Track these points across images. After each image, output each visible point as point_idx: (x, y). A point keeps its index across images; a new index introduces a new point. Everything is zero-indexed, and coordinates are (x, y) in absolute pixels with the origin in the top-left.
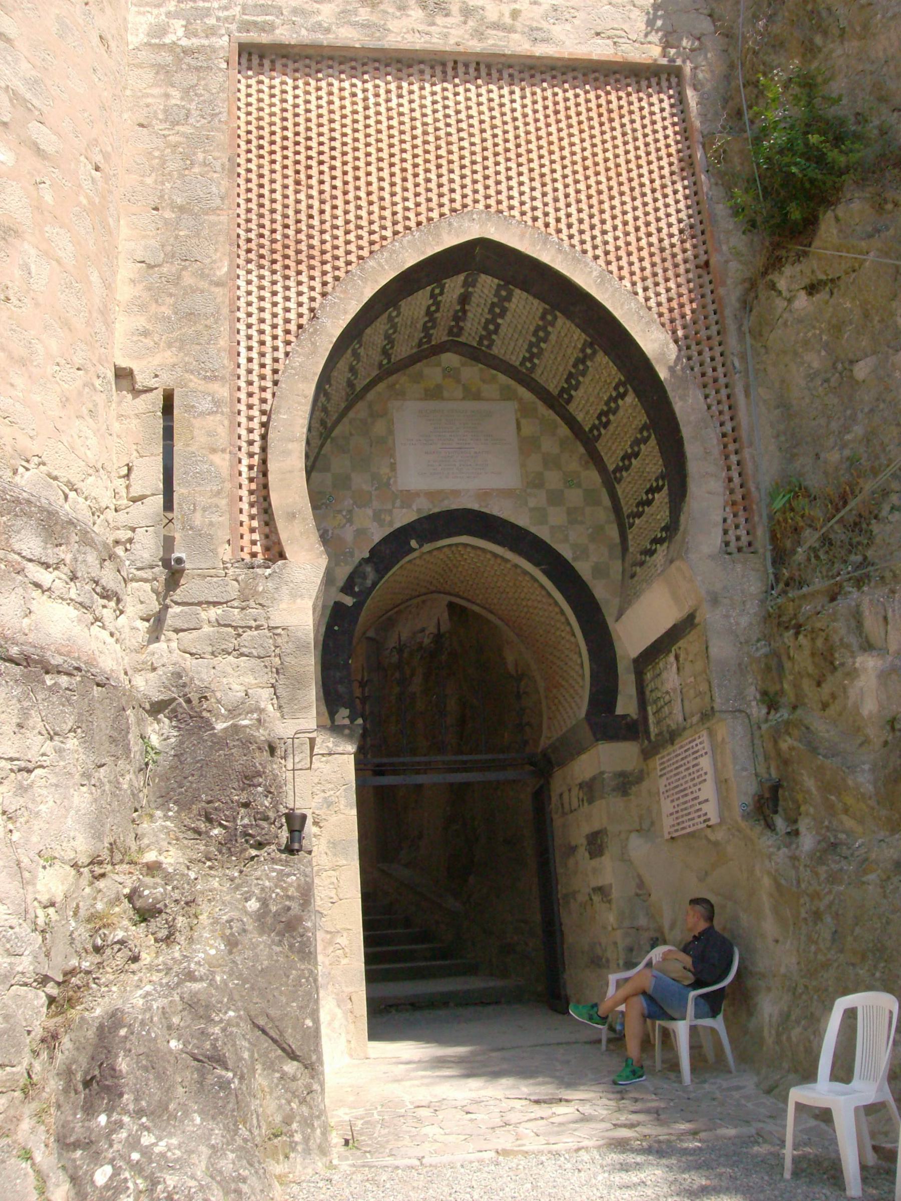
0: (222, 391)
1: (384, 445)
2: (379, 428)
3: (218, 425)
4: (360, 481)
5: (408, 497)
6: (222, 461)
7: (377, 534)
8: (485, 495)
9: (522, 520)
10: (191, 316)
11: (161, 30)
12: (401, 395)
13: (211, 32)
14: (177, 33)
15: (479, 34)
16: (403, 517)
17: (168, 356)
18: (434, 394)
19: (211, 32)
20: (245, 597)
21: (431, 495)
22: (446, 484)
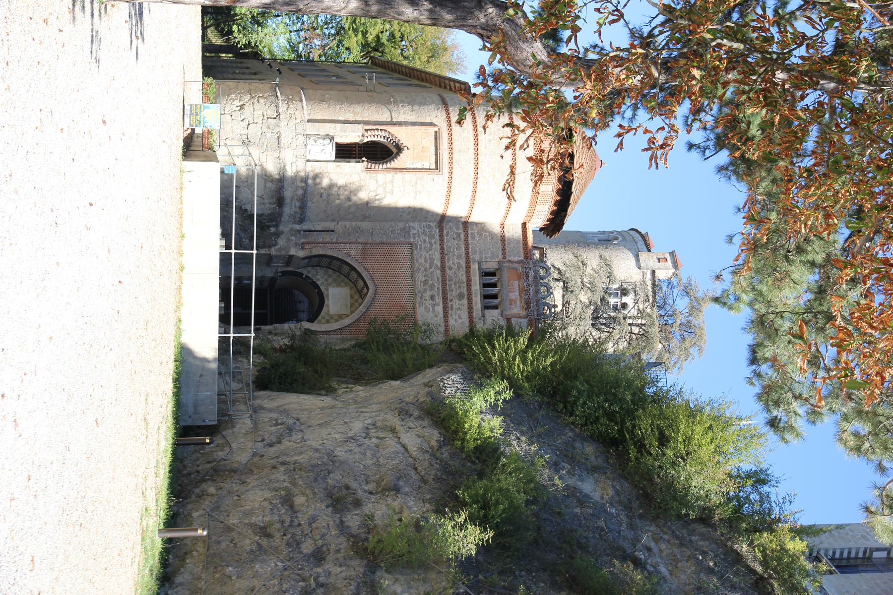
0: (334, 240)
1: (339, 285)
2: (343, 284)
3: (328, 240)
4: (330, 280)
5: (327, 290)
6: (321, 240)
7: (318, 283)
8: (328, 306)
9: (322, 314)
10: (349, 235)
11: (413, 228)
12: (351, 289)
13: (414, 238)
14: (413, 231)
15: (419, 292)
16: (322, 288)
17: (341, 231)
18: (352, 297)
19: (414, 238)
20: (296, 244)
21: (328, 295)
22: (330, 298)
